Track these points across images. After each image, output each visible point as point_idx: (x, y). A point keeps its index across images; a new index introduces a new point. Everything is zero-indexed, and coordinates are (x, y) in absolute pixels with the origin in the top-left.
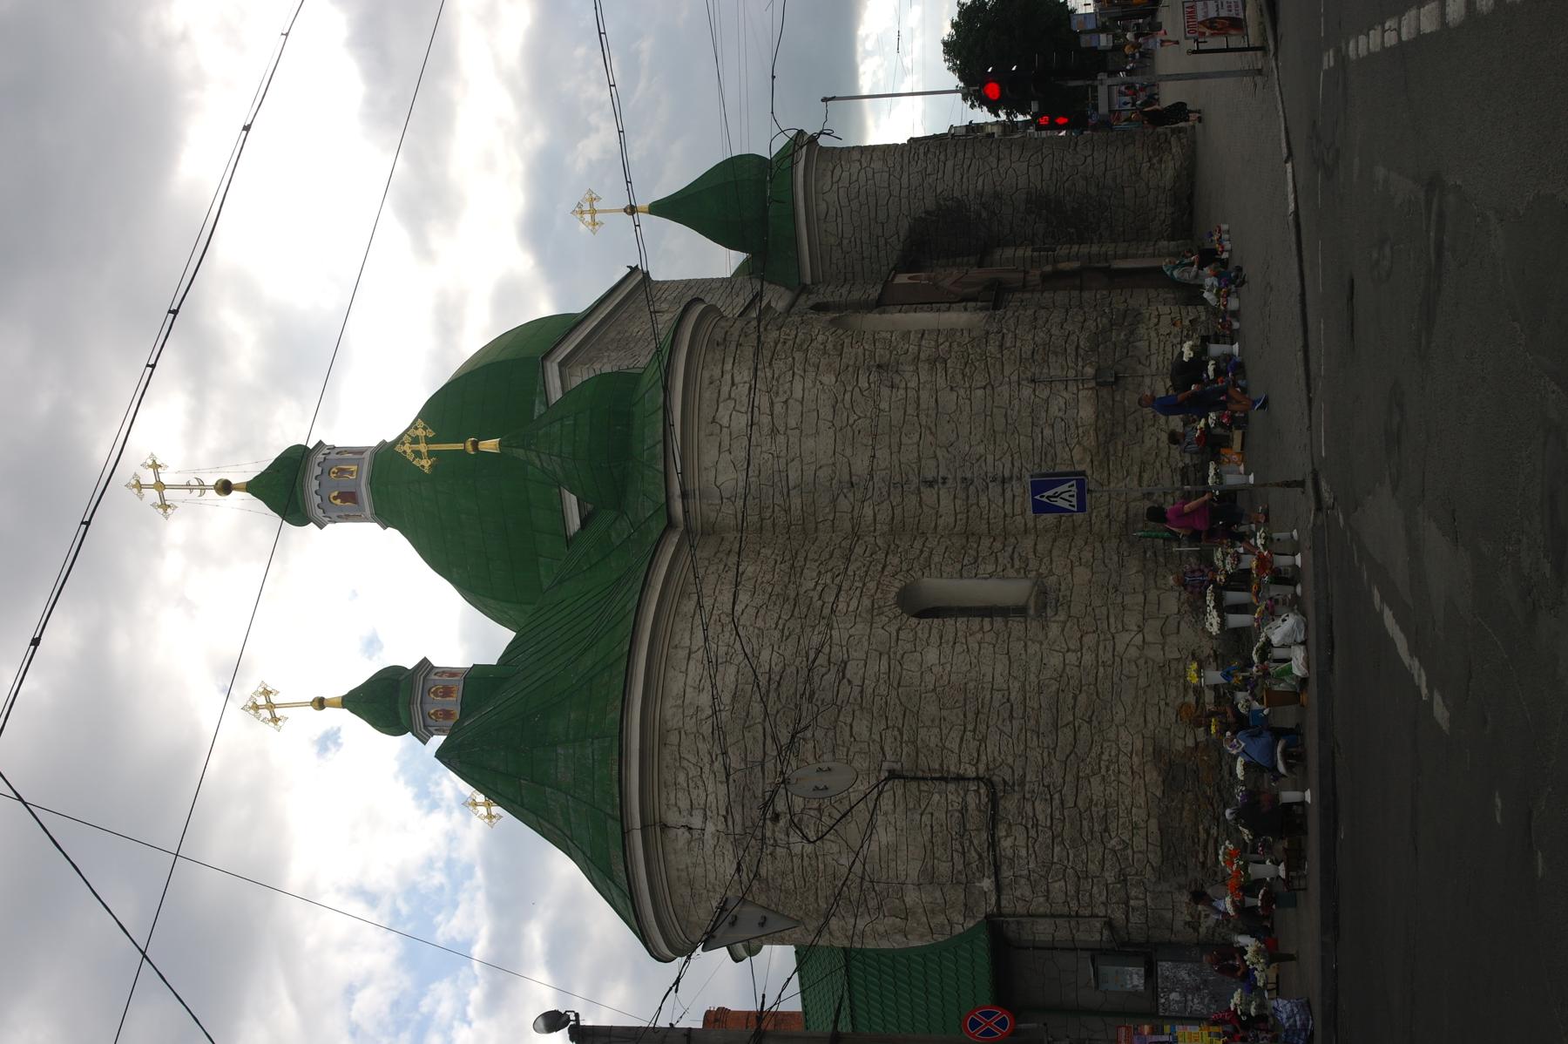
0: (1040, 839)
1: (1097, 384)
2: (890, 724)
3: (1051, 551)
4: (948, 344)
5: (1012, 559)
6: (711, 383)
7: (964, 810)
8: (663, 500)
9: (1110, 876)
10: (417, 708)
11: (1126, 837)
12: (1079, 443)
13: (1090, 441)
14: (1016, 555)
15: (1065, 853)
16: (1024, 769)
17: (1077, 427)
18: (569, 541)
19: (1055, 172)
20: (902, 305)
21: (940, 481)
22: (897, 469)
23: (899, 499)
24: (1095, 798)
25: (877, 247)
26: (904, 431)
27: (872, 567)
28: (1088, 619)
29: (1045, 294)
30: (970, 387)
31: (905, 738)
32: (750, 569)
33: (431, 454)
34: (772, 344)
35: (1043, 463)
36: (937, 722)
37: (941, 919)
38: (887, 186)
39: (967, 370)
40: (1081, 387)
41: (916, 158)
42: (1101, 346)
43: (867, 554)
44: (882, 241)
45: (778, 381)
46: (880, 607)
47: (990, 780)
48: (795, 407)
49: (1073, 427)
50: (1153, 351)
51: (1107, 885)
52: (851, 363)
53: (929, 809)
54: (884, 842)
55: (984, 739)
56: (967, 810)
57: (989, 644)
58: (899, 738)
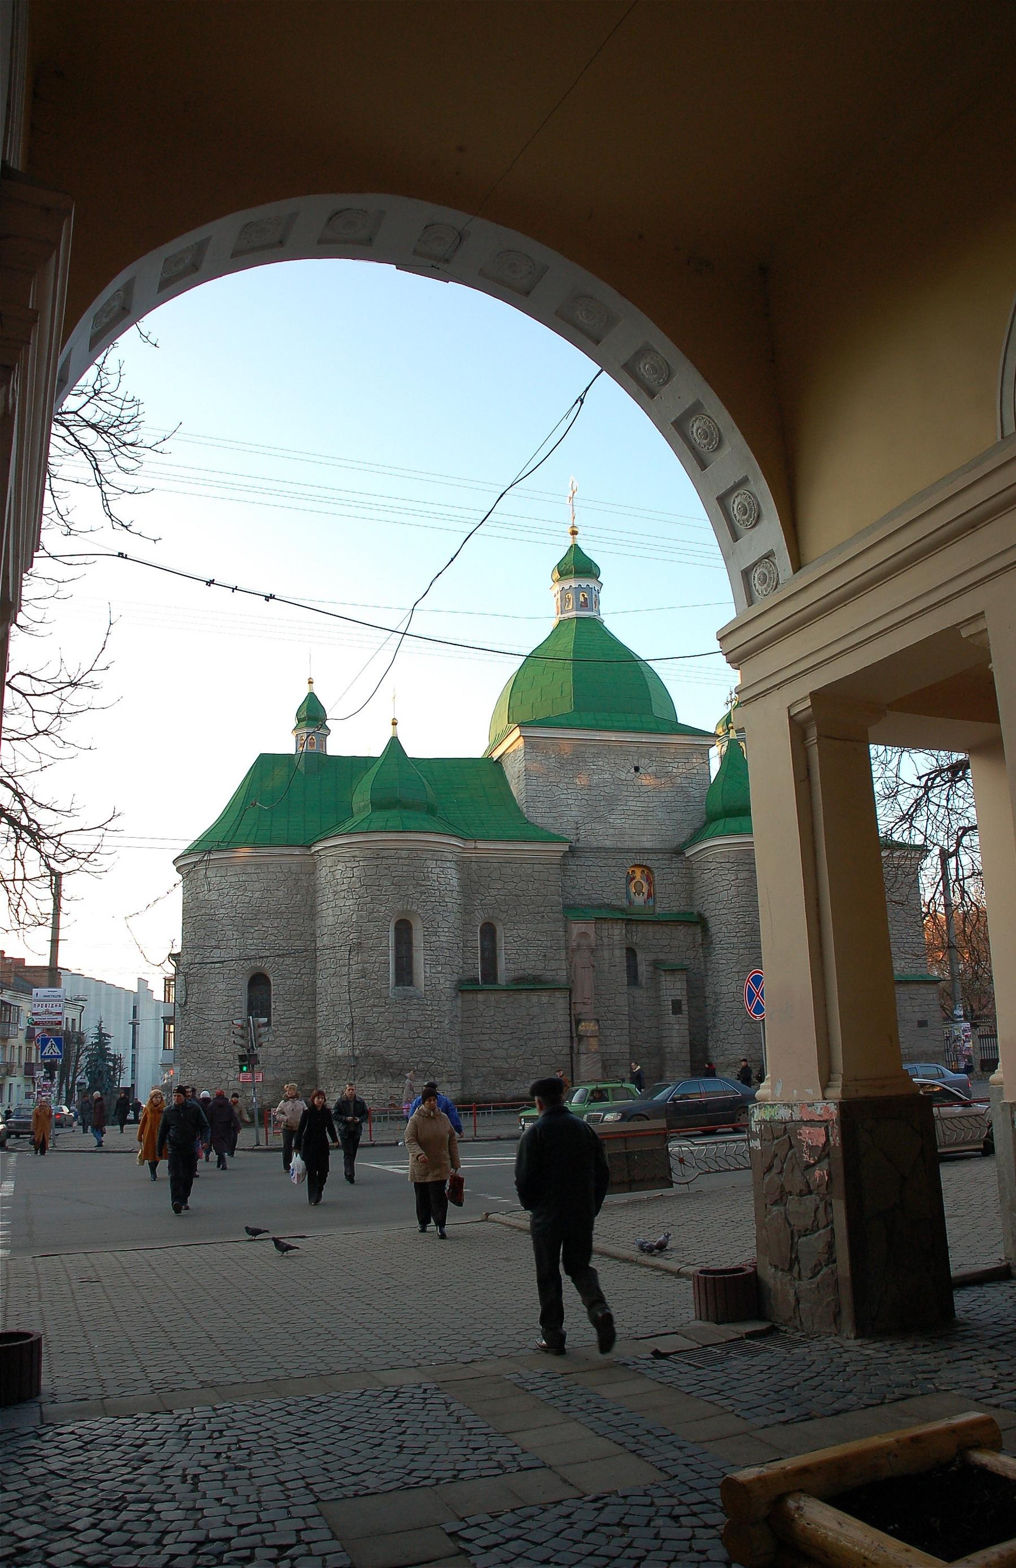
14: (292, 1019)
41: (740, 916)
42: (372, 1058)
44: (703, 900)
45: (354, 891)
52: (363, 928)
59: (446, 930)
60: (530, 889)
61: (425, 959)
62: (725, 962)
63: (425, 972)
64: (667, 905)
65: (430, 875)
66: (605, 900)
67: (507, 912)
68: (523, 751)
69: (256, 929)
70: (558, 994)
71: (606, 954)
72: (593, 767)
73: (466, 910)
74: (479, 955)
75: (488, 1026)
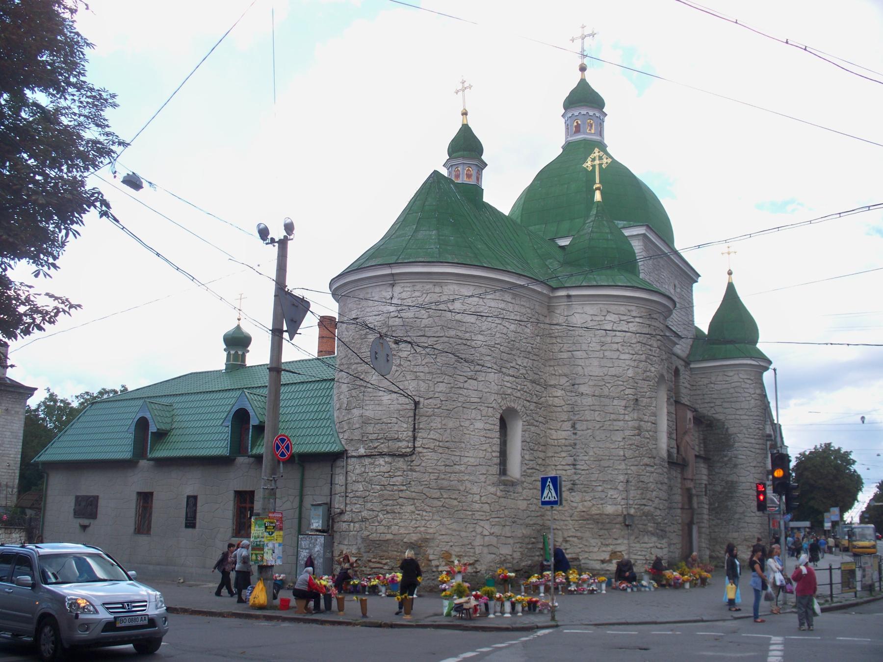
0: (383, 479)
1: (625, 515)
2: (443, 402)
3: (536, 489)
4: (649, 437)
5: (532, 469)
6: (629, 311)
7: (398, 440)
8: (566, 285)
9: (365, 514)
10: (460, 161)
11: (384, 522)
12: (594, 505)
13: (594, 511)
14: (534, 471)
15: (376, 491)
16: (419, 471)
17: (602, 504)
18: (553, 240)
19: (747, 496)
20: (676, 415)
21: (575, 431)
22: (581, 409)
23: (565, 410)
24: (404, 507)
25: (709, 403)
26: (601, 413)
27: (528, 395)
28: (498, 507)
29: (679, 490)
31: (436, 410)
33: (594, 166)
34: (650, 343)
35: (583, 486)
36: (443, 427)
37: (346, 427)
38: (742, 407)
39: (634, 447)
40: (624, 506)
43: (536, 393)
44: (712, 405)
45: (630, 346)
46: (506, 398)
47: (414, 453)
48: (615, 355)
49: (602, 502)
50: (642, 545)
51: (360, 512)
52: (638, 385)
53: (399, 422)
54: (383, 398)
55: (434, 451)
56: (398, 441)
57: (485, 455)
58: (436, 407)
69: (512, 365)
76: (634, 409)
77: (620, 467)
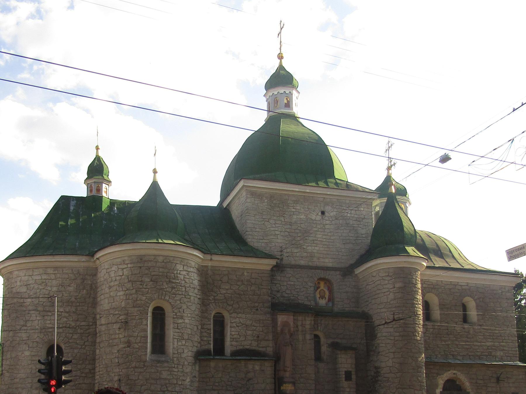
4: (138, 347)
14: (77, 377)
19: (387, 379)
30: (119, 357)
32: (71, 289)
44: (367, 303)
45: (124, 285)
52: (129, 312)
59: (189, 315)
60: (249, 290)
61: (174, 335)
62: (383, 345)
63: (173, 344)
64: (342, 306)
65: (179, 276)
66: (300, 301)
67: (232, 306)
68: (245, 197)
70: (267, 364)
71: (301, 337)
72: (293, 210)
73: (204, 303)
74: (212, 335)
75: (217, 384)
76: (125, 329)
77: (115, 371)
